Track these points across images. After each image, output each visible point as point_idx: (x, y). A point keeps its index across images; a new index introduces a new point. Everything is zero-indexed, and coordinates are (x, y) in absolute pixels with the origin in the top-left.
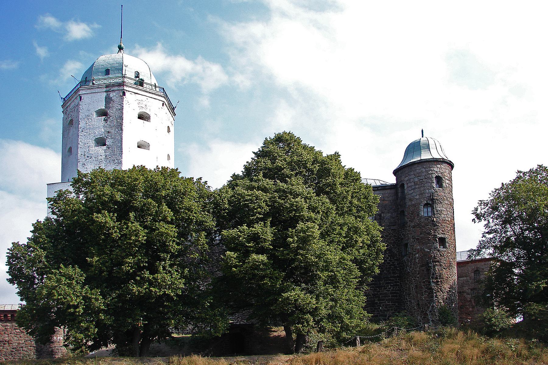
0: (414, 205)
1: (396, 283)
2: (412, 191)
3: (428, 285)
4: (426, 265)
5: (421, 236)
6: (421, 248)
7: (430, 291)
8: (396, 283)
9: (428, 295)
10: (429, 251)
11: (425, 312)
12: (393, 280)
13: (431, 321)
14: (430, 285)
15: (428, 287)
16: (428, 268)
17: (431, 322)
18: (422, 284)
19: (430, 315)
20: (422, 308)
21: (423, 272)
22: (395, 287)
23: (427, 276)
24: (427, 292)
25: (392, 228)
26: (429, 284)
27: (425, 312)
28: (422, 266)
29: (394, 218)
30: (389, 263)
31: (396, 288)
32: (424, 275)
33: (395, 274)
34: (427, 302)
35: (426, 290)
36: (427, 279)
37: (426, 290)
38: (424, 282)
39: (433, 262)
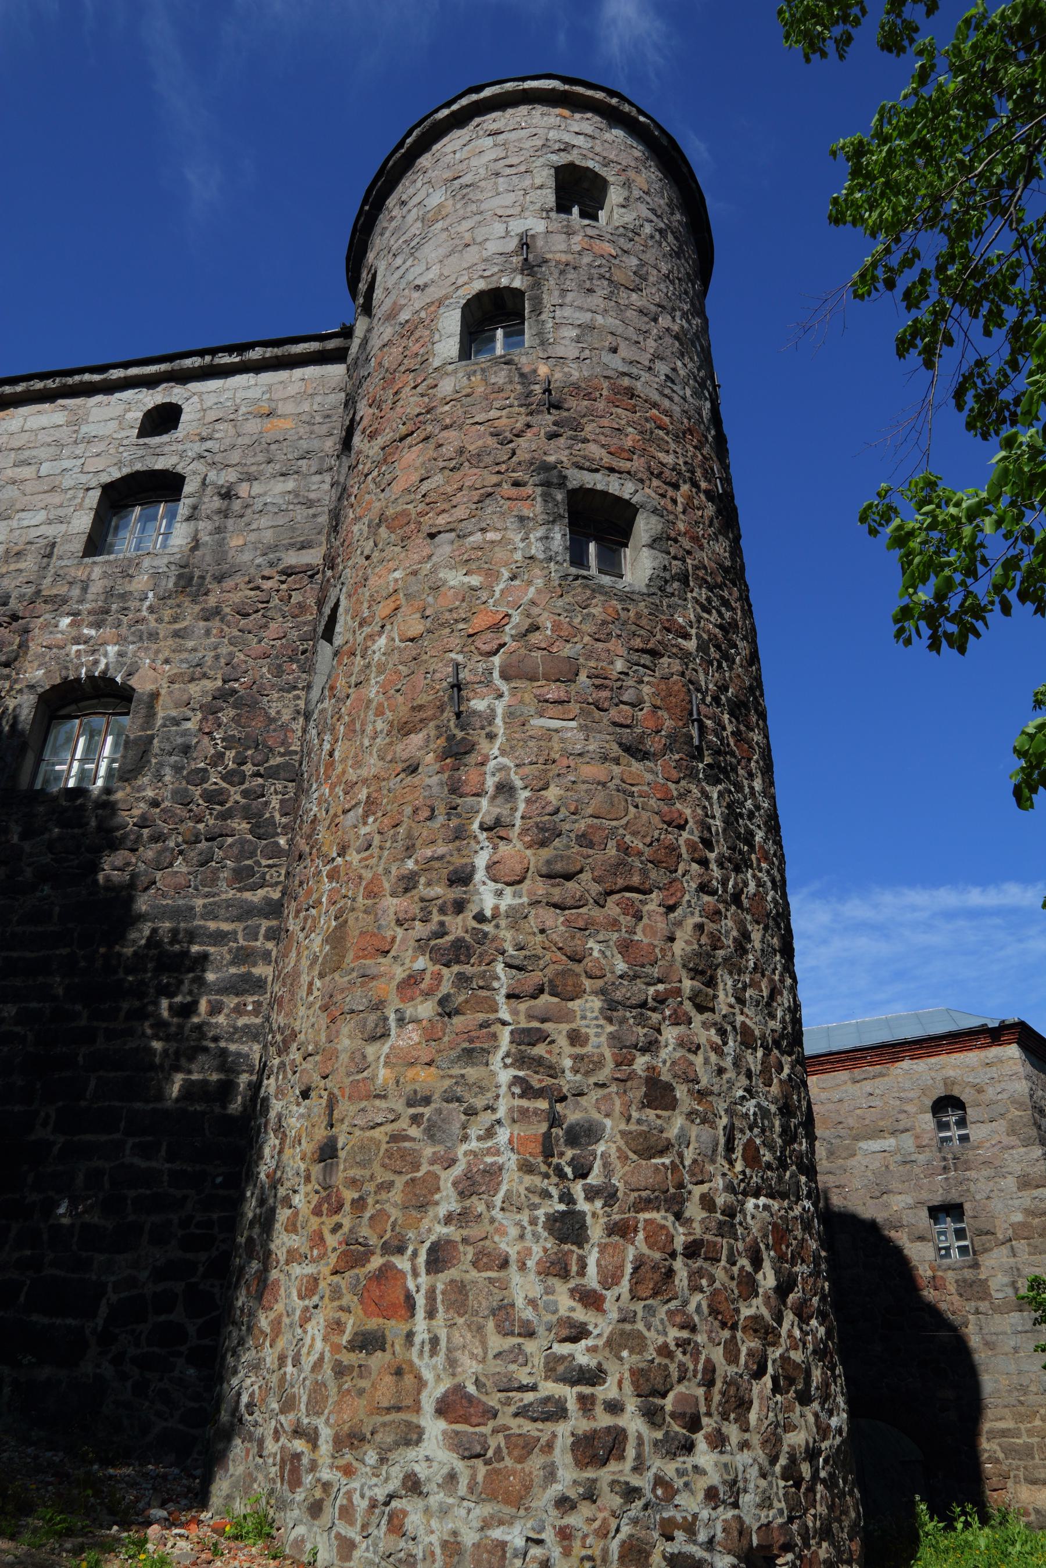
0: (408, 330)
1: (243, 969)
2: (409, 263)
3: (442, 911)
4: (442, 709)
5: (425, 487)
6: (415, 573)
7: (462, 979)
8: (243, 969)
9: (431, 1037)
10: (475, 580)
11: (376, 1262)
12: (220, 937)
13: (443, 1410)
14: (459, 907)
15: (441, 932)
16: (460, 735)
17: (434, 1427)
18: (392, 905)
19: (431, 1314)
20: (359, 1204)
21: (415, 780)
22: (231, 1001)
23: (441, 809)
24: (428, 994)
25: (292, 559)
26: (456, 893)
27: (376, 1262)
28: (405, 729)
29: (309, 504)
30: (214, 797)
31: (239, 1009)
32: (415, 811)
33: (253, 888)
34: (415, 1119)
35: (421, 962)
36: (441, 850)
37: (421, 962)
38: (408, 884)
39: (505, 676)
